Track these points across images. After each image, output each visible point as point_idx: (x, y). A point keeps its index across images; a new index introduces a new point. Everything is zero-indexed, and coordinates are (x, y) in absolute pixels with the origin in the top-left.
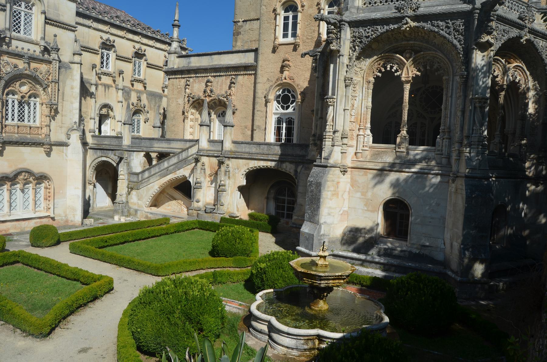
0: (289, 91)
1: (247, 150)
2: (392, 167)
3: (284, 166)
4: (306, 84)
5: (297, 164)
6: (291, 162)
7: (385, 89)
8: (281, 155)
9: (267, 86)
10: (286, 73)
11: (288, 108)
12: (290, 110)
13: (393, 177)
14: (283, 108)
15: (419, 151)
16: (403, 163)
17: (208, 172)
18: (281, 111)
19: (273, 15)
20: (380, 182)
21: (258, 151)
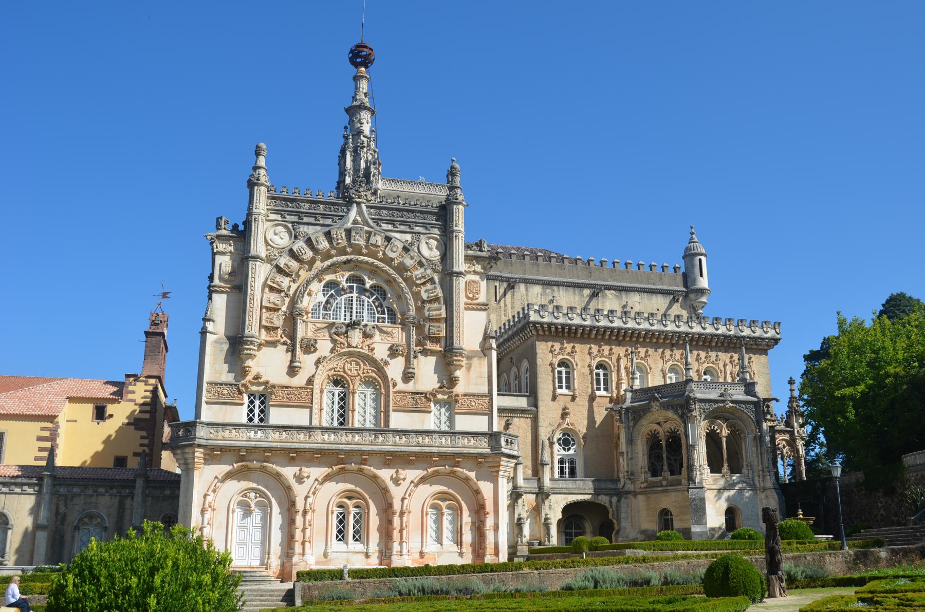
0: (569, 435)
1: (564, 486)
2: (725, 489)
3: (600, 498)
4: (584, 431)
5: (611, 495)
6: (606, 495)
7: (712, 439)
8: (595, 489)
9: (550, 430)
10: (567, 420)
11: (569, 449)
12: (571, 452)
13: (726, 494)
14: (564, 449)
15: (735, 477)
16: (729, 486)
17: (526, 508)
18: (563, 452)
19: (550, 369)
20: (719, 498)
21: (574, 486)
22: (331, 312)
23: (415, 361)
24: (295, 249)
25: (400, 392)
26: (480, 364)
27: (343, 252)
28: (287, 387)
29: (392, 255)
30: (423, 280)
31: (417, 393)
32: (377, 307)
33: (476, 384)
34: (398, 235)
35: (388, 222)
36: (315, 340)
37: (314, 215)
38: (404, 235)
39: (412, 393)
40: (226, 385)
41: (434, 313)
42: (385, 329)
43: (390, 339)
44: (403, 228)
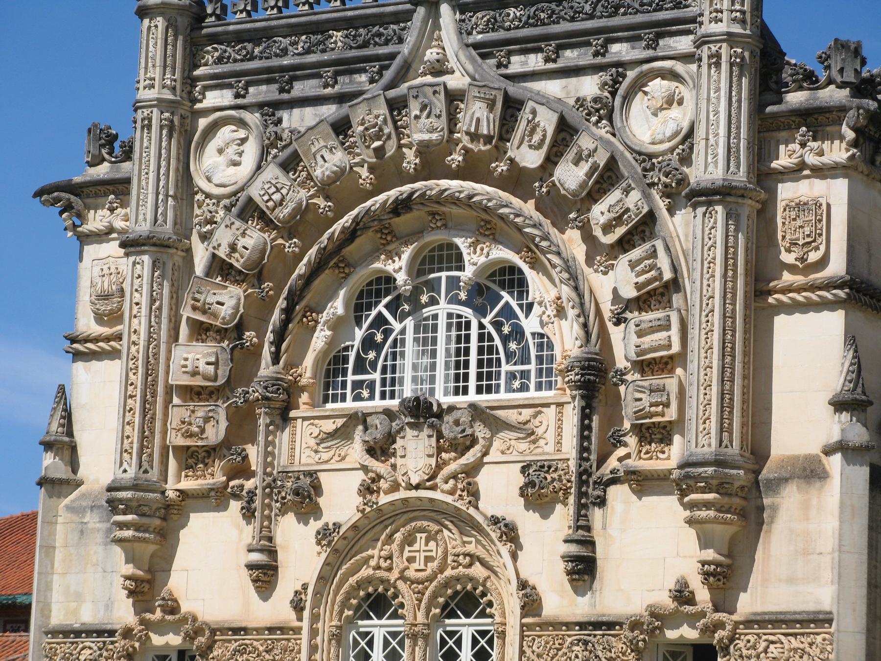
22: (377, 376)
23: (597, 514)
24: (255, 191)
25: (545, 625)
26: (806, 506)
27: (387, 172)
28: (236, 631)
29: (531, 159)
30: (620, 231)
31: (597, 625)
32: (505, 340)
33: (791, 580)
34: (553, 88)
35: (528, 46)
36: (311, 474)
37: (313, 71)
38: (573, 81)
39: (583, 625)
40: (89, 633)
41: (648, 341)
42: (511, 416)
43: (523, 446)
44: (570, 57)
